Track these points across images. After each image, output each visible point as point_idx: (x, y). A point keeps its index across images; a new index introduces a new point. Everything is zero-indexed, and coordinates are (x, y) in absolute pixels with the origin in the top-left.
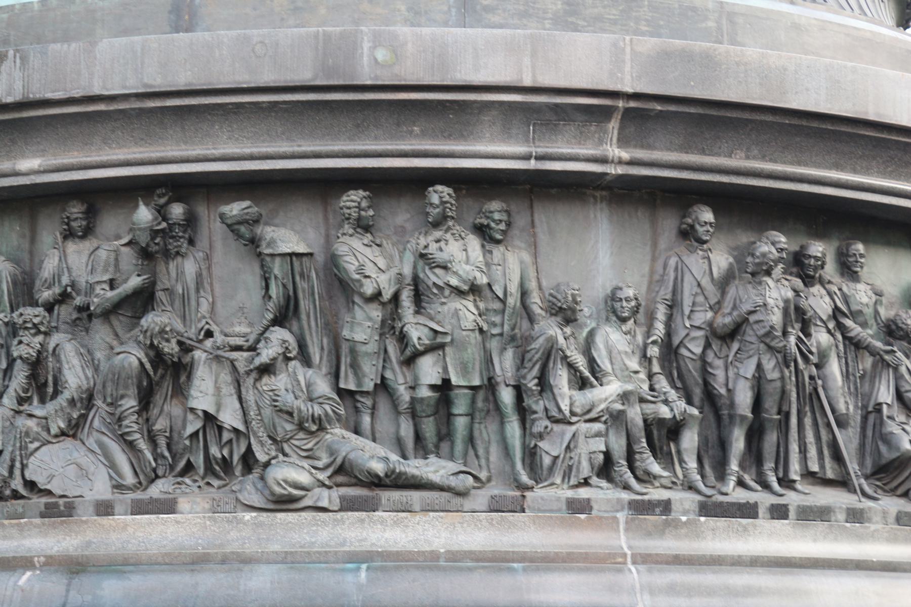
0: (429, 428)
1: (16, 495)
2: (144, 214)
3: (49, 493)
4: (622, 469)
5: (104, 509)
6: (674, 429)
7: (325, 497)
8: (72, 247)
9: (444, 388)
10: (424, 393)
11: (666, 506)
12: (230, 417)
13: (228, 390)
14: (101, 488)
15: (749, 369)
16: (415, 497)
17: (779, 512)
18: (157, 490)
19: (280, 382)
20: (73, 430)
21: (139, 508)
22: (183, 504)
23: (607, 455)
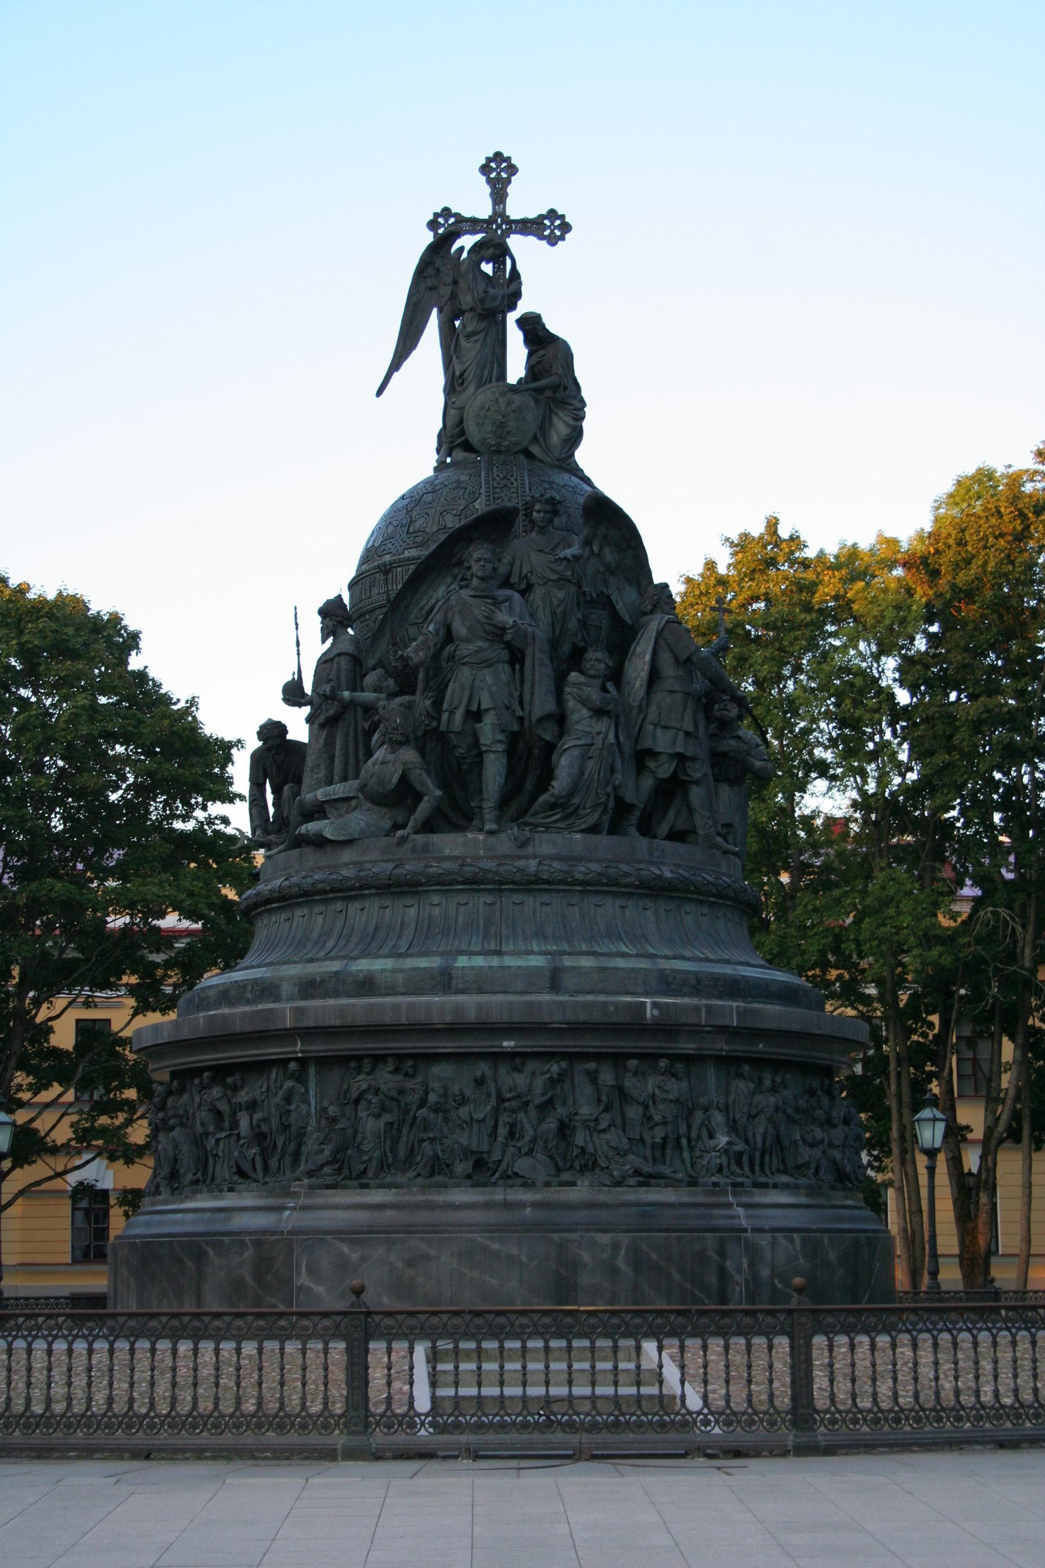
0: (658, 1154)
1: (509, 1177)
2: (555, 1068)
3: (523, 1177)
4: (725, 1170)
5: (548, 1184)
6: (739, 1155)
7: (632, 1181)
8: (516, 1075)
9: (665, 1139)
10: (658, 1140)
11: (742, 1185)
12: (590, 1149)
13: (588, 1138)
14: (541, 1176)
15: (761, 1129)
16: (662, 1181)
17: (775, 1186)
18: (565, 1176)
19: (608, 1136)
20: (530, 1153)
21: (562, 1184)
22: (579, 1183)
23: (721, 1165)
